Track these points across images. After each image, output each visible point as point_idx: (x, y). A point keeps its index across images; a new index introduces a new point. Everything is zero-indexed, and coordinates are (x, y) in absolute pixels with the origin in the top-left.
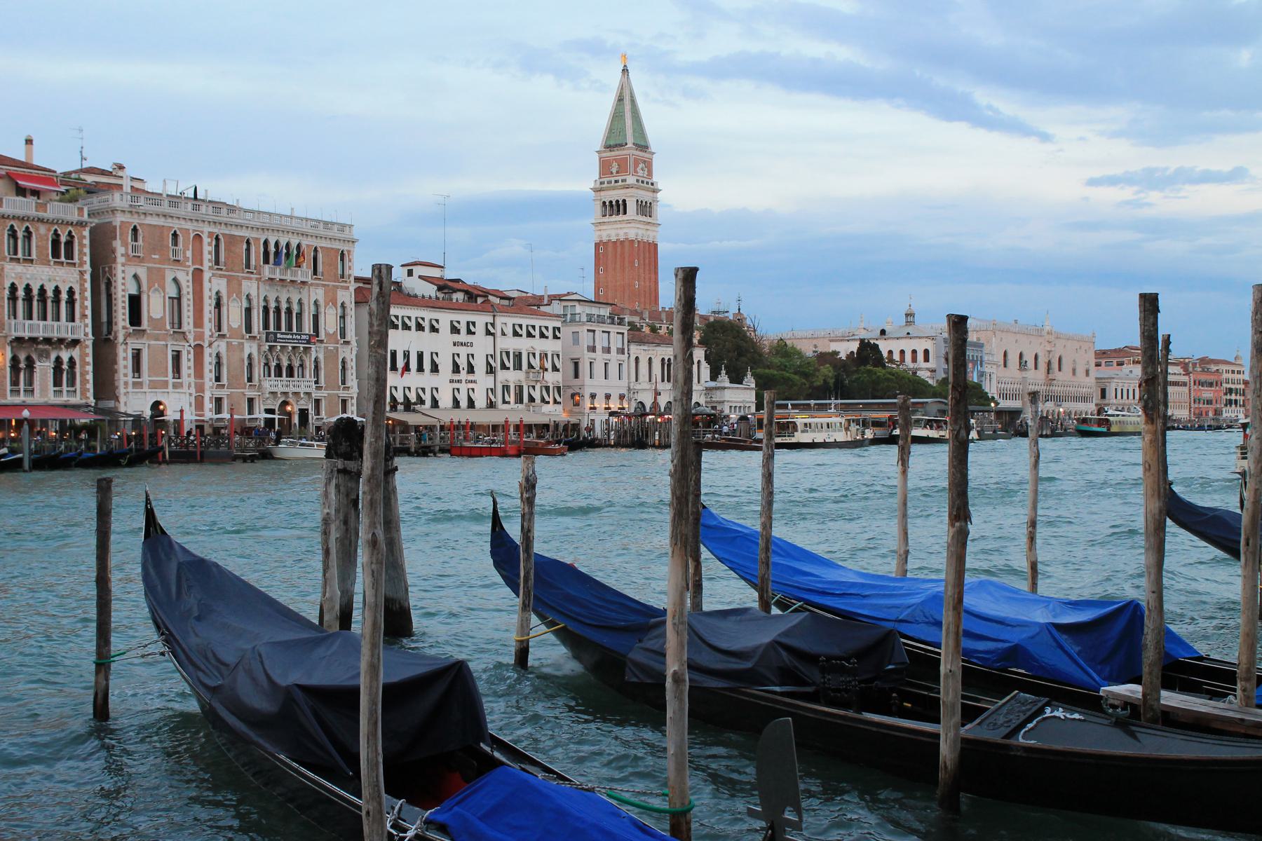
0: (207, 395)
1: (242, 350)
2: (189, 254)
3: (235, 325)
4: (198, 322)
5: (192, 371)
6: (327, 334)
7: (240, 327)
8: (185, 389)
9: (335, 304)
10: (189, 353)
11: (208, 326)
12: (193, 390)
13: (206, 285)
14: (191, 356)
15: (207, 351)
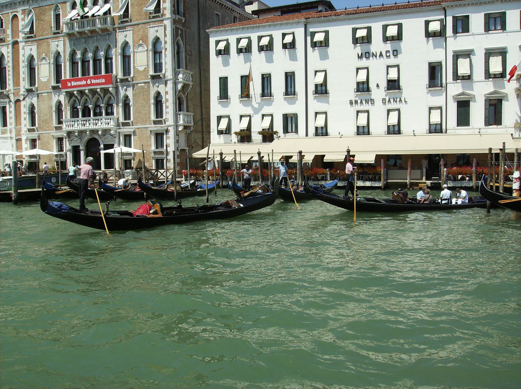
0: (24, 138)
1: (50, 99)
2: (9, 32)
3: (44, 80)
4: (17, 83)
5: (13, 121)
6: (136, 71)
7: (49, 80)
8: (8, 135)
9: (146, 42)
10: (10, 107)
11: (24, 84)
12: (13, 135)
13: (21, 52)
14: (13, 109)
15: (23, 103)
